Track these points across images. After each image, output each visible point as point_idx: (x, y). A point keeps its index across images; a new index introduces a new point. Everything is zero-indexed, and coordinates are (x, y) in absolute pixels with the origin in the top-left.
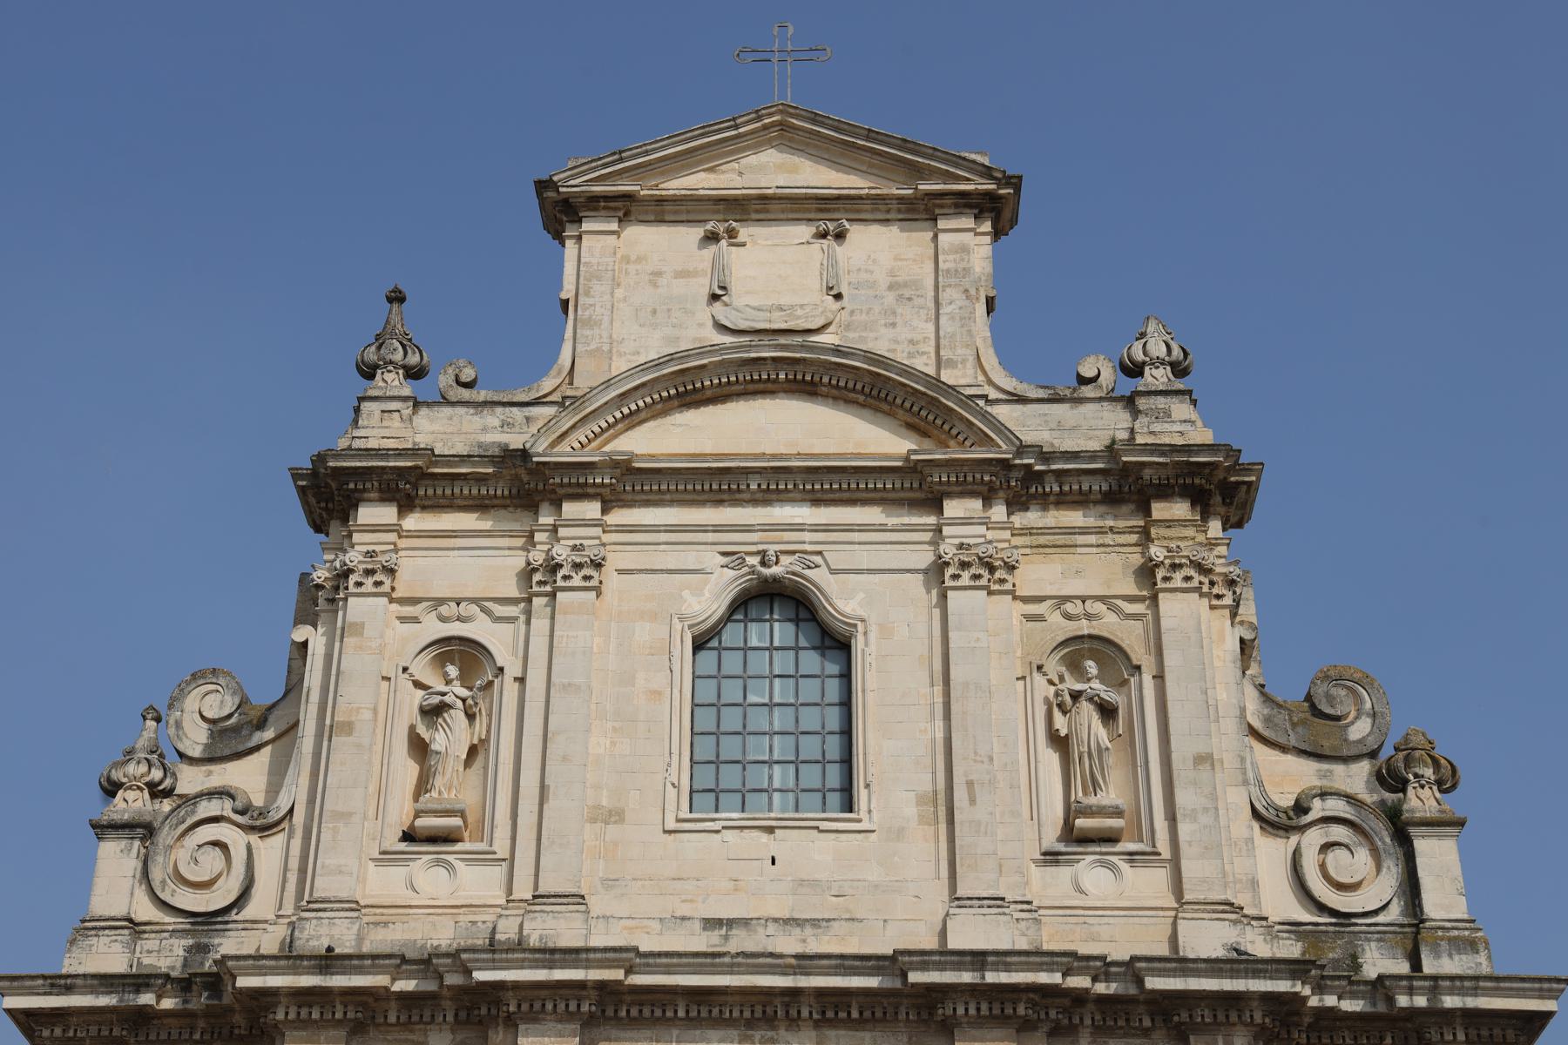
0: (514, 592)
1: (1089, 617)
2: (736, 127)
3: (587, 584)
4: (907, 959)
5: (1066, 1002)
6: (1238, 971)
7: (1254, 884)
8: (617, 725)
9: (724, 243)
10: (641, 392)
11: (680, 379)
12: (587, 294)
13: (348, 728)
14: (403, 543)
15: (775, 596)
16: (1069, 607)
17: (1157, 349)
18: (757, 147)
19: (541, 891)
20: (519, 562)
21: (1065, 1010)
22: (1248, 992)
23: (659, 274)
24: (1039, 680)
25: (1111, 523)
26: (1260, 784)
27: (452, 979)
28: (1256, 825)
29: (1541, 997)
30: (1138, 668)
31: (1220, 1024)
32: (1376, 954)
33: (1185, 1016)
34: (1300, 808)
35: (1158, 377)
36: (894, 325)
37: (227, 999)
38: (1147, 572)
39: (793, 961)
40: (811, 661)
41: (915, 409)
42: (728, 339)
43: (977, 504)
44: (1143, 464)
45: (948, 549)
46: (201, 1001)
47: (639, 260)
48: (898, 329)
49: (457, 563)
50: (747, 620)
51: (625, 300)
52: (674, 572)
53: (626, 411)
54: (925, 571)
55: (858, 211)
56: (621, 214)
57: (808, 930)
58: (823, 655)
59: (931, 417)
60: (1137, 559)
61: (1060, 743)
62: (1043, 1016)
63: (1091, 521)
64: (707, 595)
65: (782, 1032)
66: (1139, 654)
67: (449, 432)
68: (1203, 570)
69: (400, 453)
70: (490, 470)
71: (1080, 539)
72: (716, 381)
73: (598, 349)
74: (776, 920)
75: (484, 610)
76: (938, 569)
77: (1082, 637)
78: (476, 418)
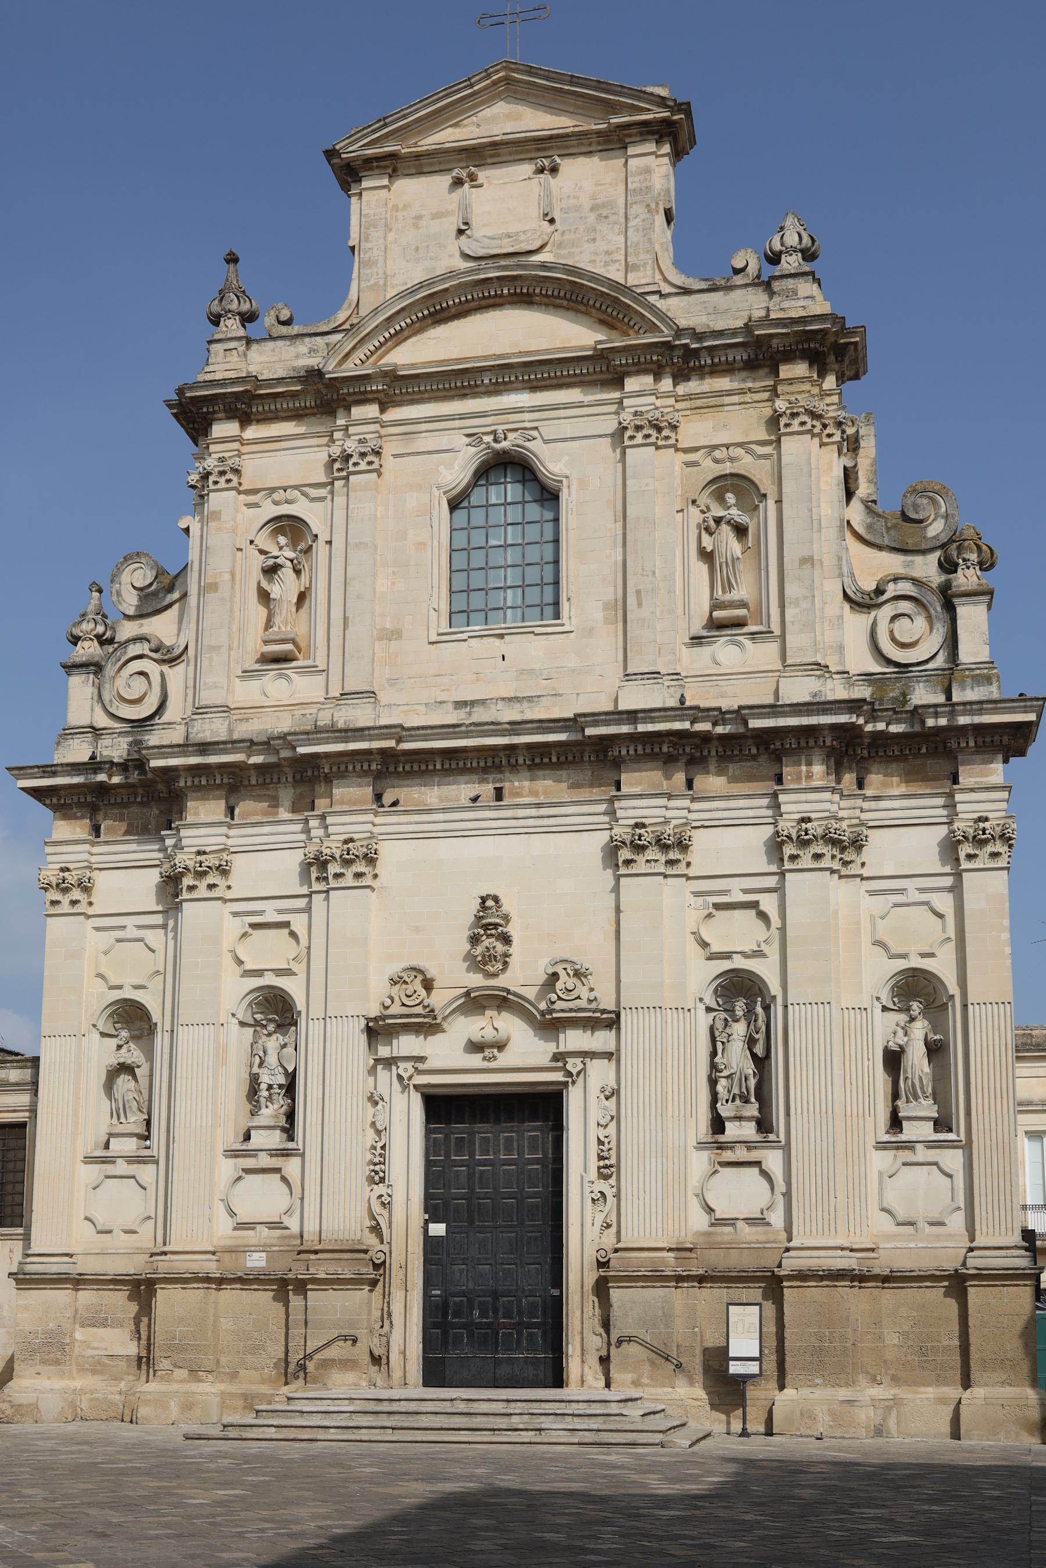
0: (323, 479)
1: (732, 459)
2: (471, 86)
3: (370, 468)
4: (583, 719)
5: (697, 741)
6: (812, 711)
7: (841, 648)
8: (395, 569)
9: (466, 186)
10: (403, 314)
11: (430, 302)
12: (367, 240)
13: (214, 587)
14: (245, 449)
15: (506, 465)
16: (717, 454)
17: (792, 239)
18: (490, 101)
19: (346, 691)
20: (323, 456)
21: (697, 747)
22: (819, 725)
23: (419, 217)
24: (694, 511)
25: (750, 385)
26: (853, 575)
27: (285, 754)
28: (847, 606)
29: (1026, 712)
30: (765, 496)
31: (803, 748)
32: (923, 691)
33: (778, 744)
34: (879, 591)
35: (791, 262)
36: (594, 240)
37: (150, 776)
38: (774, 421)
39: (507, 726)
40: (534, 511)
41: (603, 307)
42: (471, 264)
43: (649, 379)
44: (771, 335)
46: (135, 777)
47: (405, 207)
48: (597, 244)
49: (281, 458)
50: (489, 484)
51: (395, 241)
52: (434, 451)
53: (392, 331)
54: (612, 435)
55: (567, 147)
56: (390, 171)
57: (525, 704)
58: (542, 506)
59: (615, 313)
60: (768, 412)
61: (707, 556)
62: (681, 751)
63: (736, 385)
64: (456, 468)
65: (507, 774)
66: (766, 485)
67: (273, 361)
68: (814, 415)
69: (234, 381)
70: (299, 388)
71: (727, 400)
72: (457, 301)
73: (376, 284)
74: (503, 699)
75: (304, 494)
76: (619, 434)
77: (725, 475)
78: (292, 348)
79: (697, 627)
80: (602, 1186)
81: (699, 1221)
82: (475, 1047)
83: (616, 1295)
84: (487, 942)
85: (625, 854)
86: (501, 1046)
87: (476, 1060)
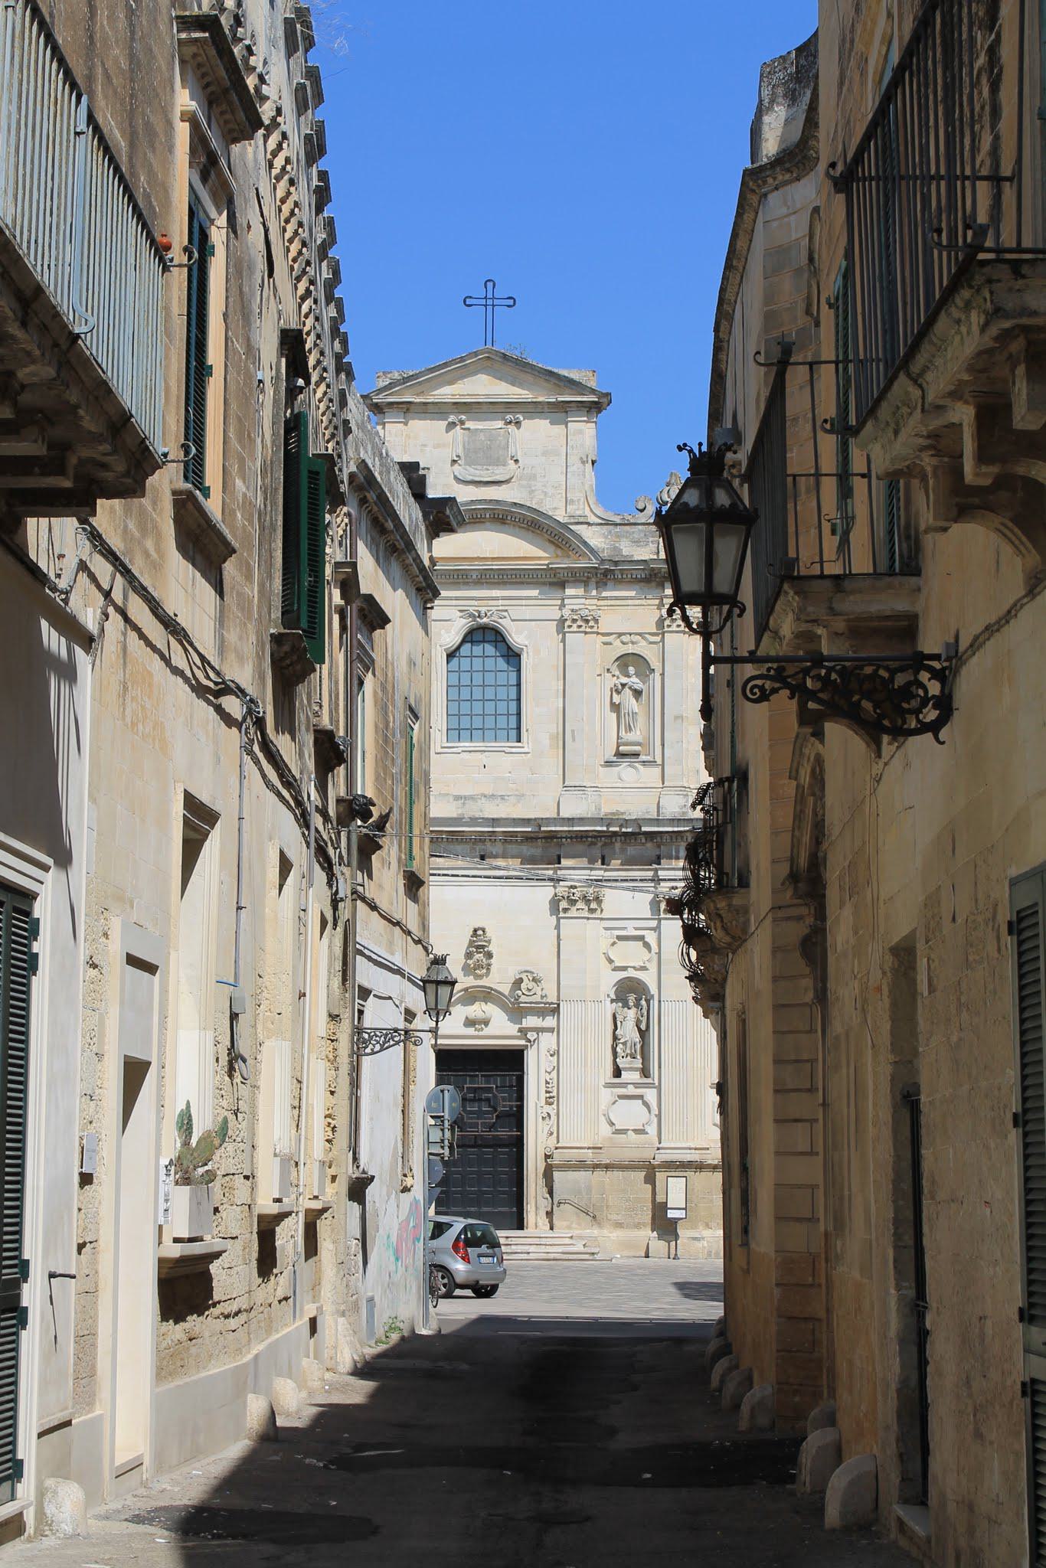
1: (633, 643)
15: (484, 633)
16: (624, 638)
40: (502, 664)
45: (566, 612)
61: (616, 708)
66: (655, 664)
76: (562, 621)
79: (610, 754)
81: (605, 1130)
82: (470, 1023)
83: (556, 1174)
84: (477, 956)
85: (563, 904)
86: (486, 1023)
87: (471, 1031)
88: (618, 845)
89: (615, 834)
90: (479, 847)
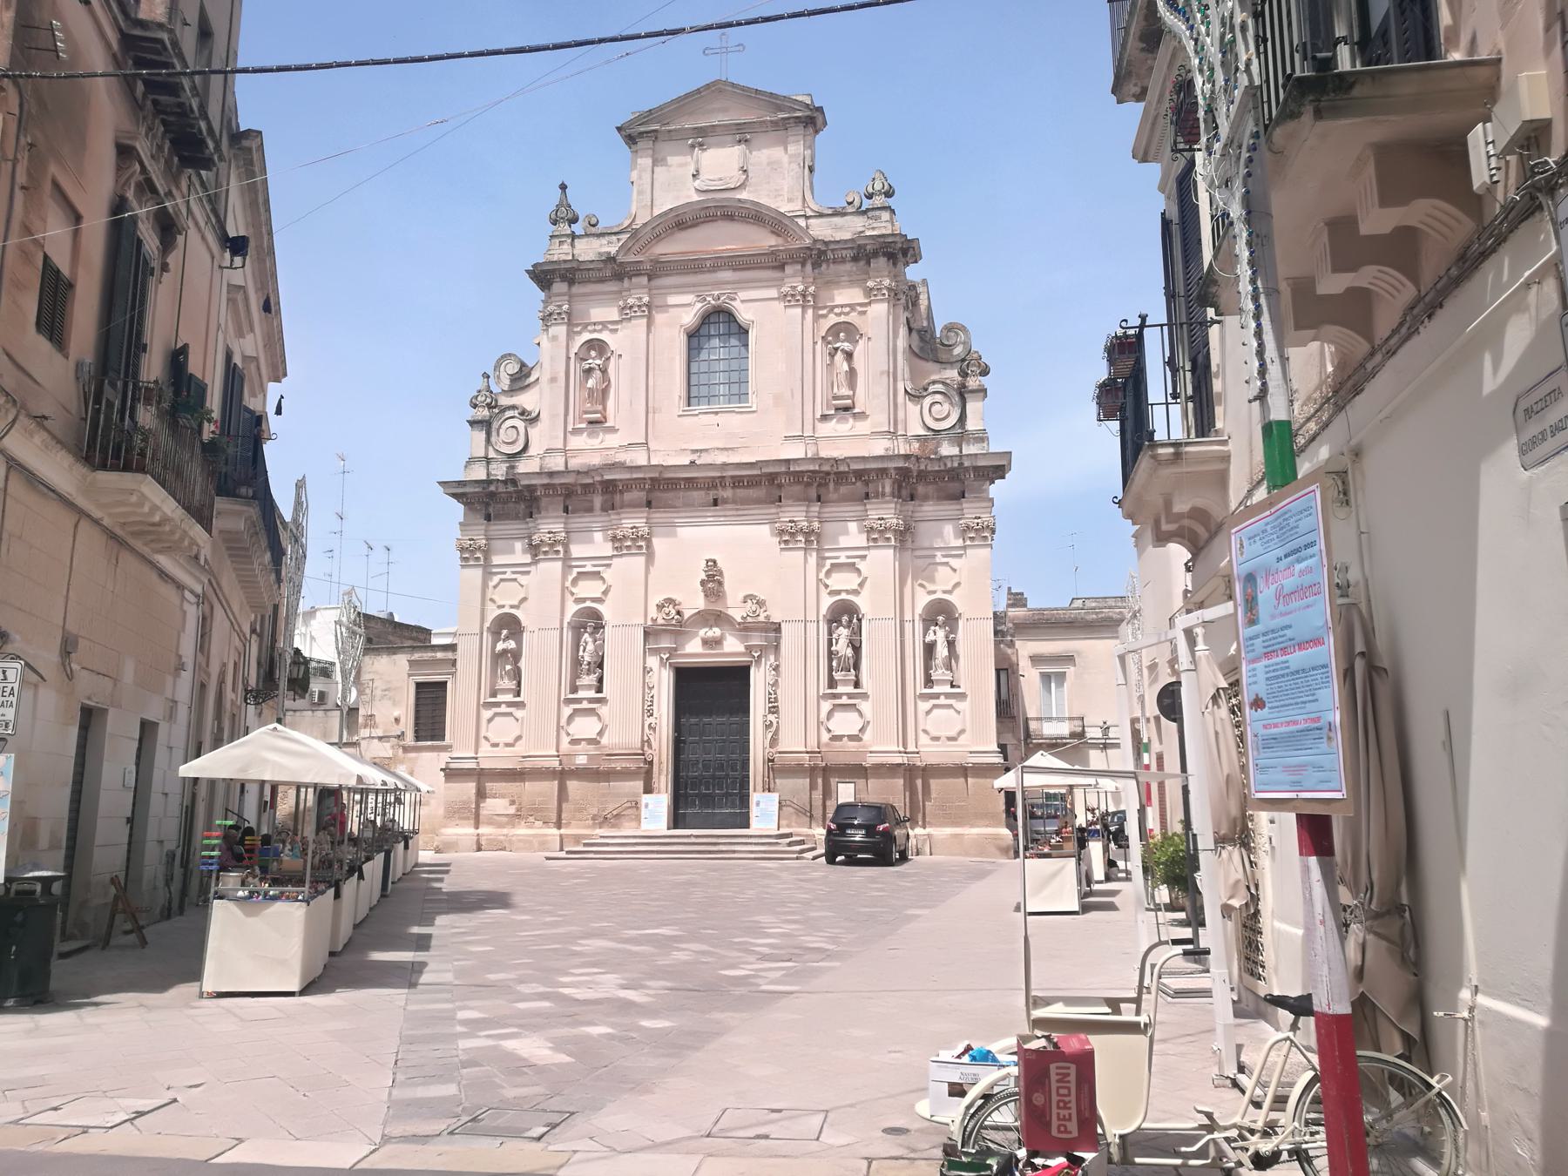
27: (598, 478)
80: (771, 717)
84: (710, 585)
88: (831, 485)
89: (828, 473)
90: (712, 494)
